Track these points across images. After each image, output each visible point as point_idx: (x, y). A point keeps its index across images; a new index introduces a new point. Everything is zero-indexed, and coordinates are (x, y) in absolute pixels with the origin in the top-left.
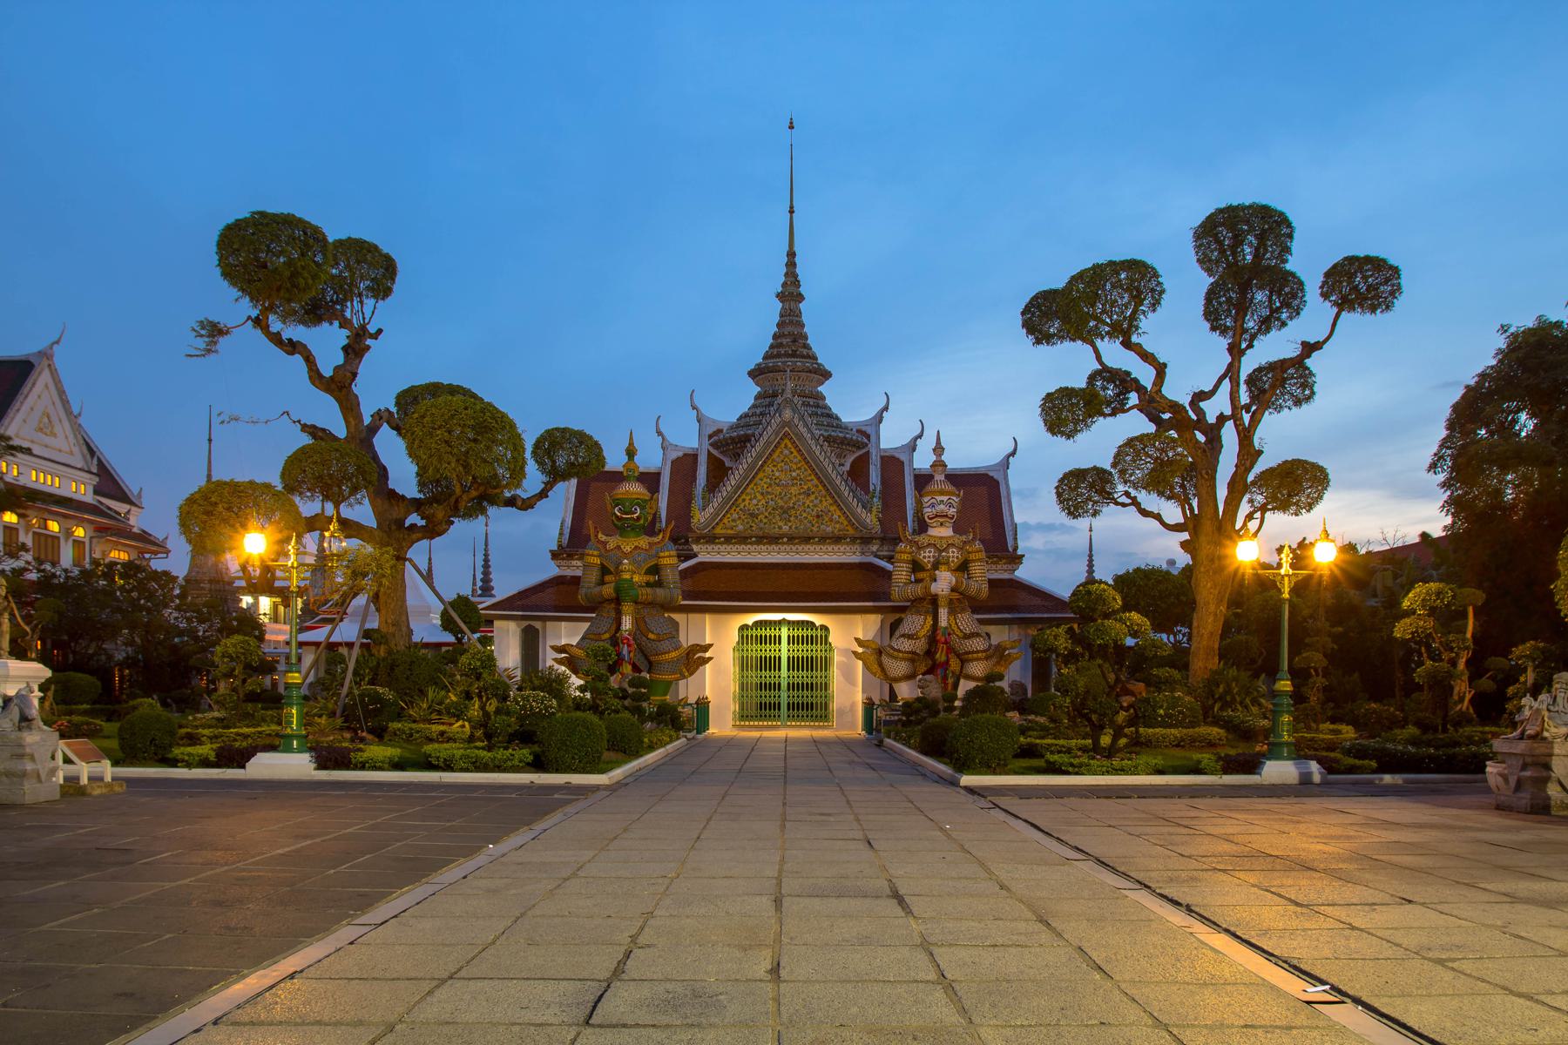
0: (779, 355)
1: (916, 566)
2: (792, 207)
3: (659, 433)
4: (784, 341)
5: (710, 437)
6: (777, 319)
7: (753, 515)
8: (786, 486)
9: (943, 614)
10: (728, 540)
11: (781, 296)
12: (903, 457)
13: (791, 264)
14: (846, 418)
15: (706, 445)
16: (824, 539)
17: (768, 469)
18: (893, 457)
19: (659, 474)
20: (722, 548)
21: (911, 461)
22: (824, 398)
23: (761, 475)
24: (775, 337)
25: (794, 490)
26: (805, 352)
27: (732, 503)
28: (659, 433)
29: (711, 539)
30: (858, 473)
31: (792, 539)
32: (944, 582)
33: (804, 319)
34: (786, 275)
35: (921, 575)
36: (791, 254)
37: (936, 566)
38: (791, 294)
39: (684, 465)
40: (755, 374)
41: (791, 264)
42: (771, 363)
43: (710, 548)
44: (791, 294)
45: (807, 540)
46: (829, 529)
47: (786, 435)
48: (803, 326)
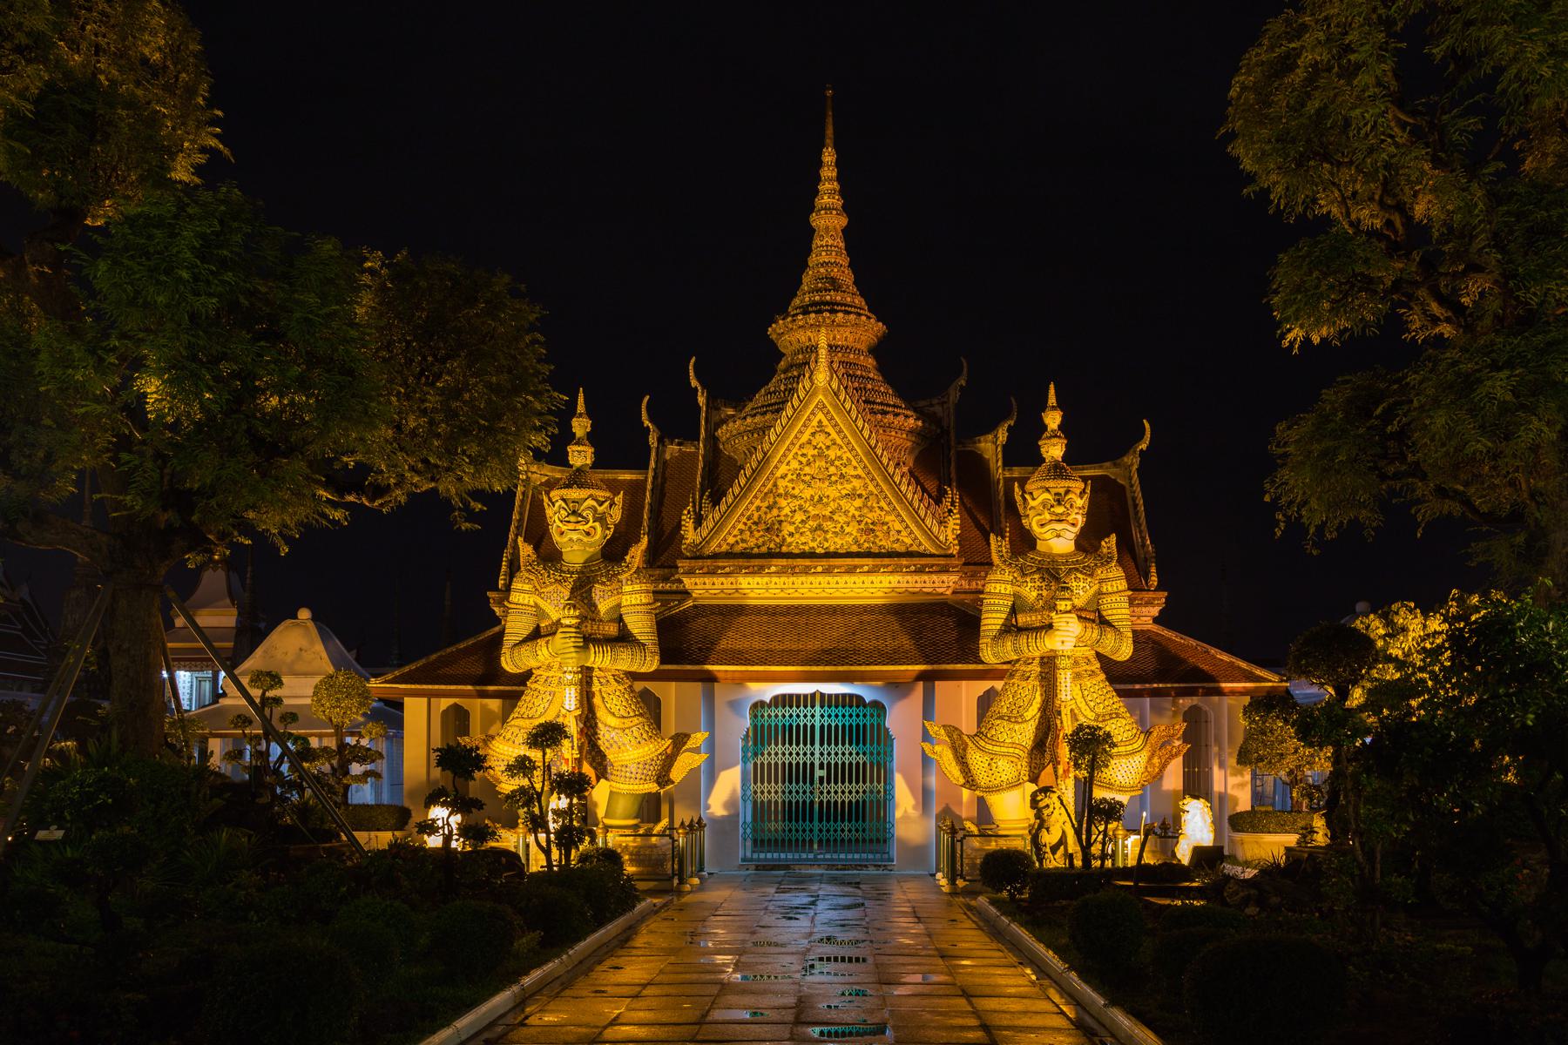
23: (783, 469)
25: (832, 492)
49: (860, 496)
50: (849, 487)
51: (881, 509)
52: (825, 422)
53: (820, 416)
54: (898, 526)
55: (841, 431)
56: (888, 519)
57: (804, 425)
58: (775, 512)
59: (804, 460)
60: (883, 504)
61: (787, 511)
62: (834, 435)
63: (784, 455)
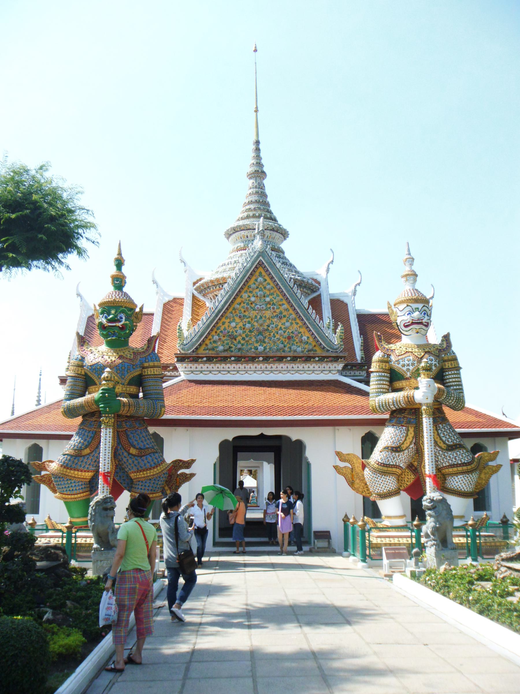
0: (248, 217)
2: (257, 108)
5: (194, 284)
9: (426, 422)
10: (210, 359)
11: (251, 176)
14: (300, 268)
15: (192, 289)
16: (294, 359)
18: (338, 300)
19: (152, 315)
22: (283, 253)
23: (239, 300)
24: (245, 205)
25: (268, 314)
27: (214, 326)
31: (266, 359)
35: (398, 384)
37: (416, 374)
42: (241, 223)
46: (299, 349)
47: (260, 264)
49: (285, 316)
50: (278, 311)
51: (297, 324)
52: (264, 273)
53: (261, 269)
54: (308, 334)
55: (272, 278)
56: (302, 330)
57: (251, 274)
58: (233, 324)
59: (251, 295)
60: (298, 321)
61: (241, 324)
62: (269, 280)
63: (240, 291)
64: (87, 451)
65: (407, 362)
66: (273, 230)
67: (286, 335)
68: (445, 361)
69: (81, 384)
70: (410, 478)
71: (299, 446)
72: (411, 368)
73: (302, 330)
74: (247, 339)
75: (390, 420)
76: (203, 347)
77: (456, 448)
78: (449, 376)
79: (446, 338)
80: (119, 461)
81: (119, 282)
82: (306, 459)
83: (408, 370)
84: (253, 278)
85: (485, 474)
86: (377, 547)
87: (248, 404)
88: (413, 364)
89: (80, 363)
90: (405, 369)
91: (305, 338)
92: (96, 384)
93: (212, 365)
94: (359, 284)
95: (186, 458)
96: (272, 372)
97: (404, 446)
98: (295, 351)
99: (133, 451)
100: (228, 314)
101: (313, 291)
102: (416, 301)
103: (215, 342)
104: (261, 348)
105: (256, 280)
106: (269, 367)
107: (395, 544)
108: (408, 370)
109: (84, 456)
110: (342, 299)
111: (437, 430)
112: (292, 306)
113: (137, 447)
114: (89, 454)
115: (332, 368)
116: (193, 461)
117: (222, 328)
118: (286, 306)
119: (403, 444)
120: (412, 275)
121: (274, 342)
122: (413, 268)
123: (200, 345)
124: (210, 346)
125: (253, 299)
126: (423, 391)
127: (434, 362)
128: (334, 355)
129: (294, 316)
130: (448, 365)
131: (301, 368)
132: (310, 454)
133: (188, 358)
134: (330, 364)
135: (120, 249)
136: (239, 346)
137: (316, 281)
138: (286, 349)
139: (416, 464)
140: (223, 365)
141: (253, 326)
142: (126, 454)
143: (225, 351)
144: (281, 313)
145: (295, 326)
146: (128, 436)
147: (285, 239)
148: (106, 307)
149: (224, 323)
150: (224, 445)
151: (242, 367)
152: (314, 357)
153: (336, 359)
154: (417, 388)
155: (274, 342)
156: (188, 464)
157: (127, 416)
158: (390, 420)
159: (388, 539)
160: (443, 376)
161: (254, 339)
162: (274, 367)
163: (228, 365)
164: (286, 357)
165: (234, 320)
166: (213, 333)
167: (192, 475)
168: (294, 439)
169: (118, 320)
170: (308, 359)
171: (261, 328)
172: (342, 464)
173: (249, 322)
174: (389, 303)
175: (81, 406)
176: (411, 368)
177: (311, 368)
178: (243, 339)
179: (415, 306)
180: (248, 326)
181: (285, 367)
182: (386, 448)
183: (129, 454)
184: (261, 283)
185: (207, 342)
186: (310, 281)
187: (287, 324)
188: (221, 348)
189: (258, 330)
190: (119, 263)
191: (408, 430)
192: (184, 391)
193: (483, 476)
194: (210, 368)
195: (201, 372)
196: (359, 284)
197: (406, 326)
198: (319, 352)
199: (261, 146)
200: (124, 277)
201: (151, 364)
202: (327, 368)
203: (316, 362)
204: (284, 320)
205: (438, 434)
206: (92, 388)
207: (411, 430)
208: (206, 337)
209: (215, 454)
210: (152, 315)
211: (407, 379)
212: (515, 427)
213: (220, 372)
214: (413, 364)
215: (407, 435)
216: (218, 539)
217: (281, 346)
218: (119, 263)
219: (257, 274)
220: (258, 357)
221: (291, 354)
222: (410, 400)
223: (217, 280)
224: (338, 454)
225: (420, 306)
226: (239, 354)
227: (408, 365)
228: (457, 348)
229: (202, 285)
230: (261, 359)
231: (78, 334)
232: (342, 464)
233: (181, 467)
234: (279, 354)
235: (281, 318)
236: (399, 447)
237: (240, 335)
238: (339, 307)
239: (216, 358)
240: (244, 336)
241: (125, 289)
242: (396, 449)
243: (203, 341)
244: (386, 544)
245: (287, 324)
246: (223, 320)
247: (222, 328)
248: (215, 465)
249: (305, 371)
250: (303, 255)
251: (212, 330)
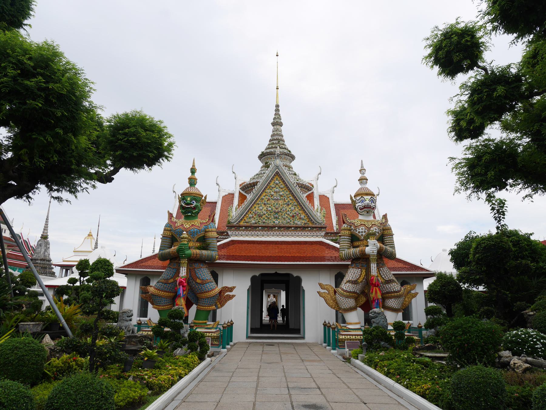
0: (272, 148)
1: (354, 239)
3: (217, 184)
4: (274, 142)
5: (240, 185)
6: (271, 133)
7: (260, 216)
8: (277, 200)
9: (374, 267)
12: (328, 196)
13: (277, 110)
16: (296, 228)
17: (267, 191)
19: (216, 203)
20: (243, 233)
21: (332, 197)
23: (264, 194)
24: (270, 141)
25: (281, 202)
26: (284, 146)
27: (249, 209)
28: (217, 184)
29: (238, 227)
30: (310, 197)
32: (372, 247)
33: (283, 133)
34: (275, 114)
35: (356, 244)
36: (277, 106)
38: (277, 123)
39: (228, 199)
40: (262, 156)
41: (277, 110)
42: (268, 151)
43: (237, 233)
44: (277, 123)
45: (288, 228)
46: (299, 223)
47: (277, 173)
48: (282, 136)
50: (287, 201)
52: (279, 179)
53: (277, 177)
55: (284, 181)
58: (261, 208)
61: (265, 208)
62: (281, 183)
64: (172, 280)
65: (361, 230)
66: (286, 155)
67: (291, 215)
68: (384, 230)
69: (168, 240)
70: (363, 300)
71: (299, 280)
72: (364, 234)
73: (300, 212)
74: (269, 217)
75: (351, 265)
76: (243, 222)
77: (391, 282)
78: (387, 239)
79: (385, 216)
80: (190, 287)
81: (192, 182)
82: (303, 287)
83: (362, 235)
84: (273, 181)
85: (408, 298)
86: (343, 341)
87: (268, 254)
88: (365, 232)
89: (169, 229)
90: (360, 234)
91: (302, 216)
92: (178, 241)
93: (248, 232)
94: (336, 186)
95: (230, 286)
96: (283, 236)
97: (360, 280)
98: (296, 224)
99: (198, 281)
100: (258, 202)
101: (309, 190)
102: (367, 194)
103: (250, 218)
104: (277, 222)
105: (274, 183)
106: (281, 233)
107: (353, 339)
108: (362, 235)
109: (170, 284)
110: (326, 195)
111: (379, 271)
112: (295, 197)
113: (201, 278)
114: (172, 283)
115: (318, 234)
116: (234, 287)
117: (254, 210)
118: (291, 198)
119: (359, 279)
120: (364, 179)
121: (284, 219)
122: (365, 175)
123: (241, 220)
124: (247, 220)
125: (273, 193)
126: (372, 247)
127: (377, 231)
128: (320, 226)
129: (296, 204)
130: (386, 232)
131: (300, 234)
132: (305, 284)
133: (234, 227)
134: (317, 232)
135: (194, 163)
136: (264, 221)
137: (311, 184)
138: (292, 223)
139: (366, 291)
140: (255, 232)
141: (272, 209)
142: (194, 282)
143: (256, 223)
144: (289, 202)
145: (297, 209)
146: (195, 272)
147: (293, 160)
148: (183, 197)
149: (255, 207)
150: (253, 279)
151: (265, 233)
152: (308, 227)
153: (321, 228)
154: (368, 246)
155: (284, 219)
156: (231, 289)
157: (195, 260)
158: (351, 265)
159: (349, 336)
160: (383, 239)
161: (272, 217)
162: (284, 233)
163: (258, 232)
164: (291, 227)
165: (261, 206)
166: (249, 213)
167: (234, 296)
168: (295, 275)
169: (191, 204)
170: (303, 228)
171: (277, 211)
172: (322, 291)
173: (270, 207)
174: (351, 196)
175: (169, 253)
176: (364, 234)
177: (306, 234)
178: (266, 217)
179: (366, 197)
180: (269, 209)
181: (290, 233)
182: (349, 281)
183: (196, 283)
184: (277, 184)
185: (245, 218)
186: (307, 184)
187: (293, 208)
188: (253, 222)
189: (275, 212)
190: (193, 171)
191: (362, 271)
192: (231, 247)
193: (406, 299)
194: (247, 233)
195: (242, 235)
196: (336, 186)
197: (360, 209)
198: (310, 225)
199: (280, 108)
200: (196, 179)
201: (210, 229)
202: (315, 234)
203: (309, 231)
204: (290, 206)
205: (380, 274)
206: (175, 244)
207: (364, 271)
208: (245, 215)
209: (247, 284)
210: (216, 203)
211: (361, 240)
212: (427, 271)
213: (252, 235)
214: (365, 232)
215: (361, 274)
216: (250, 335)
217: (289, 221)
218: (193, 171)
219: (275, 179)
220: (275, 227)
221: (295, 225)
222: (363, 254)
223: (253, 183)
224: (320, 285)
225: (369, 197)
226: (264, 225)
227: (362, 232)
228: (391, 223)
229: (245, 186)
230: (277, 228)
231: (168, 212)
232: (322, 291)
233: (227, 291)
234: (287, 225)
235: (288, 205)
236: (356, 281)
237: (264, 214)
238: (324, 199)
239: (250, 227)
240: (267, 215)
241: (196, 186)
242: (355, 282)
243: (243, 217)
244: (348, 339)
245: (293, 208)
246: (255, 206)
247: (254, 210)
248: (248, 290)
249: (302, 236)
250: (303, 170)
251: (248, 211)
